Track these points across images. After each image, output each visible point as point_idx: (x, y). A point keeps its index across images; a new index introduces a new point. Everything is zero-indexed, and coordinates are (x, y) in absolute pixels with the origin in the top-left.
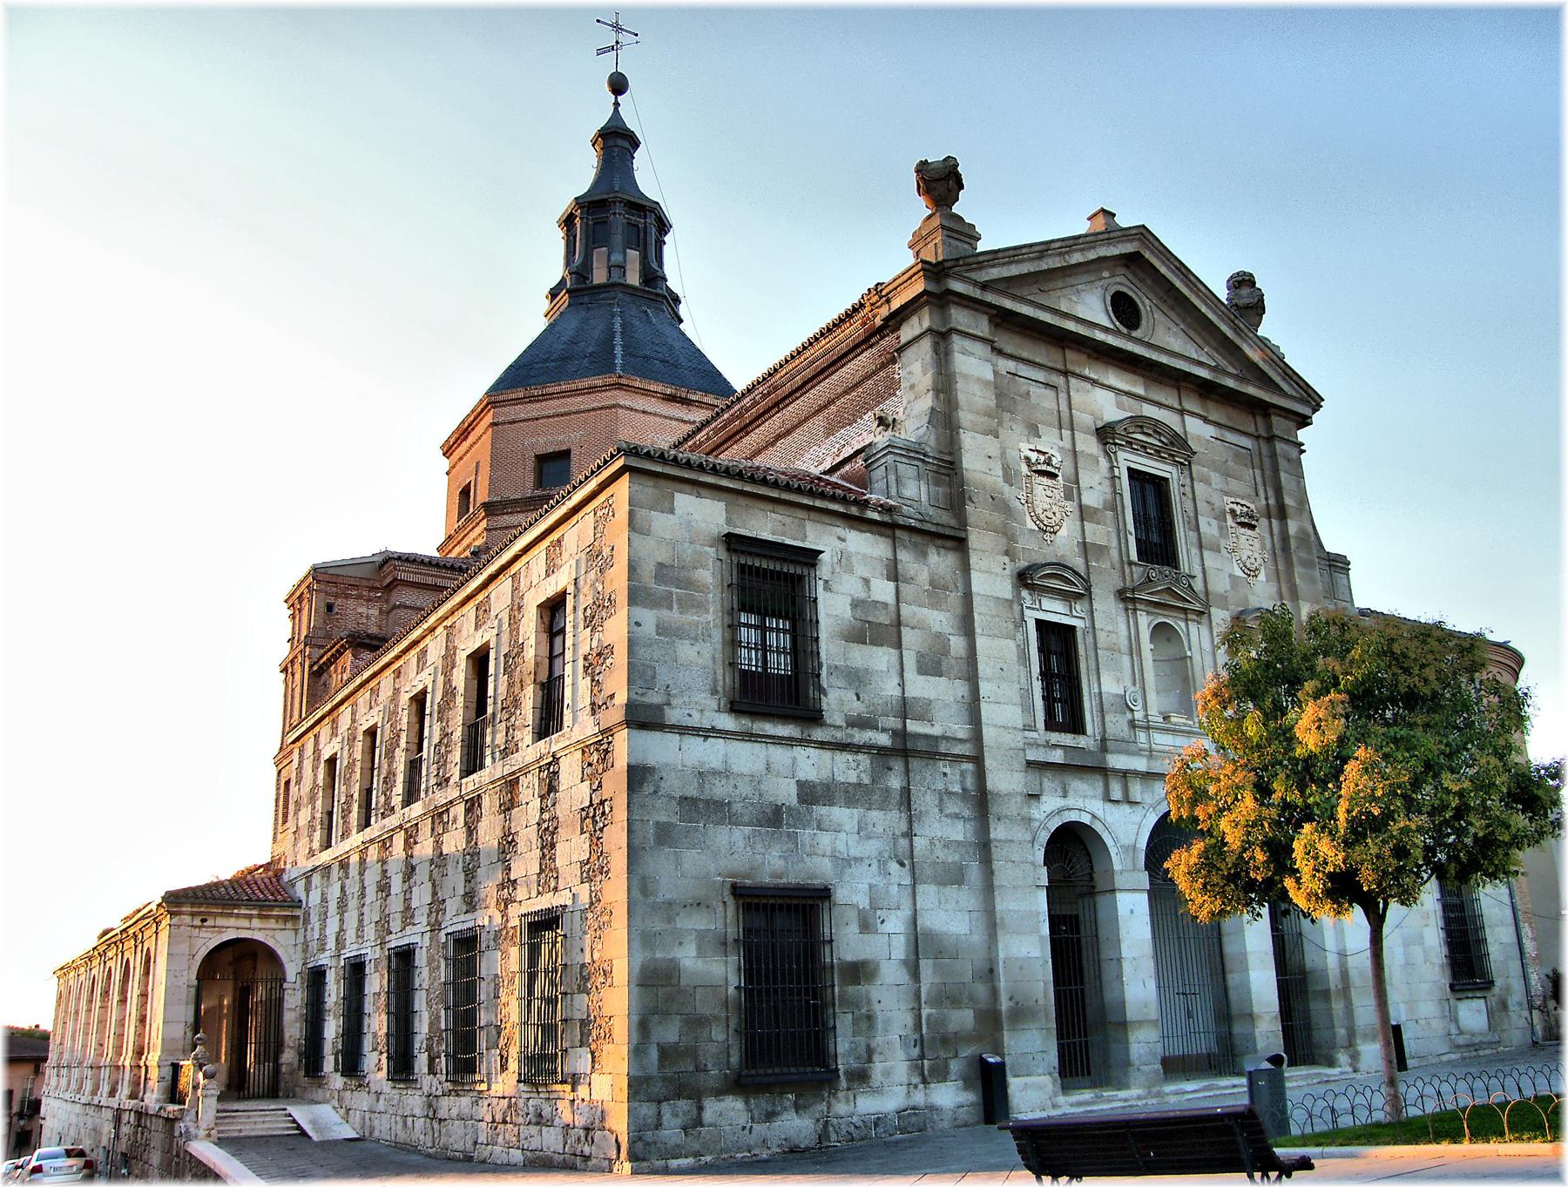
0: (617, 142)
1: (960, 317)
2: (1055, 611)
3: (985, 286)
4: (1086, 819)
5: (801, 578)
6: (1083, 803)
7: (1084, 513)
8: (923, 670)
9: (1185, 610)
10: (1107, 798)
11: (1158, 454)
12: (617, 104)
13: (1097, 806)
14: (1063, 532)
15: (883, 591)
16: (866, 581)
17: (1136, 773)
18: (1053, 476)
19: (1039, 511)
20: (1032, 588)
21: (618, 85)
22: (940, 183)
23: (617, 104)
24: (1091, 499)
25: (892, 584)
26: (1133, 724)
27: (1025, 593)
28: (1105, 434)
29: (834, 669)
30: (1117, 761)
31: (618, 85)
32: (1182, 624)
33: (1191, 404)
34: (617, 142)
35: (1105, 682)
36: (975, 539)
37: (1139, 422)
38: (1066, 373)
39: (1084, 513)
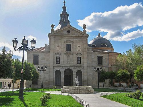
0: (64, 8)
1: (51, 37)
2: (58, 56)
6: (59, 69)
8: (46, 61)
11: (69, 43)
13: (60, 69)
15: (44, 56)
21: (64, 2)
22: (53, 26)
24: (62, 47)
30: (61, 66)
31: (64, 2)
34: (64, 8)
39: (62, 48)
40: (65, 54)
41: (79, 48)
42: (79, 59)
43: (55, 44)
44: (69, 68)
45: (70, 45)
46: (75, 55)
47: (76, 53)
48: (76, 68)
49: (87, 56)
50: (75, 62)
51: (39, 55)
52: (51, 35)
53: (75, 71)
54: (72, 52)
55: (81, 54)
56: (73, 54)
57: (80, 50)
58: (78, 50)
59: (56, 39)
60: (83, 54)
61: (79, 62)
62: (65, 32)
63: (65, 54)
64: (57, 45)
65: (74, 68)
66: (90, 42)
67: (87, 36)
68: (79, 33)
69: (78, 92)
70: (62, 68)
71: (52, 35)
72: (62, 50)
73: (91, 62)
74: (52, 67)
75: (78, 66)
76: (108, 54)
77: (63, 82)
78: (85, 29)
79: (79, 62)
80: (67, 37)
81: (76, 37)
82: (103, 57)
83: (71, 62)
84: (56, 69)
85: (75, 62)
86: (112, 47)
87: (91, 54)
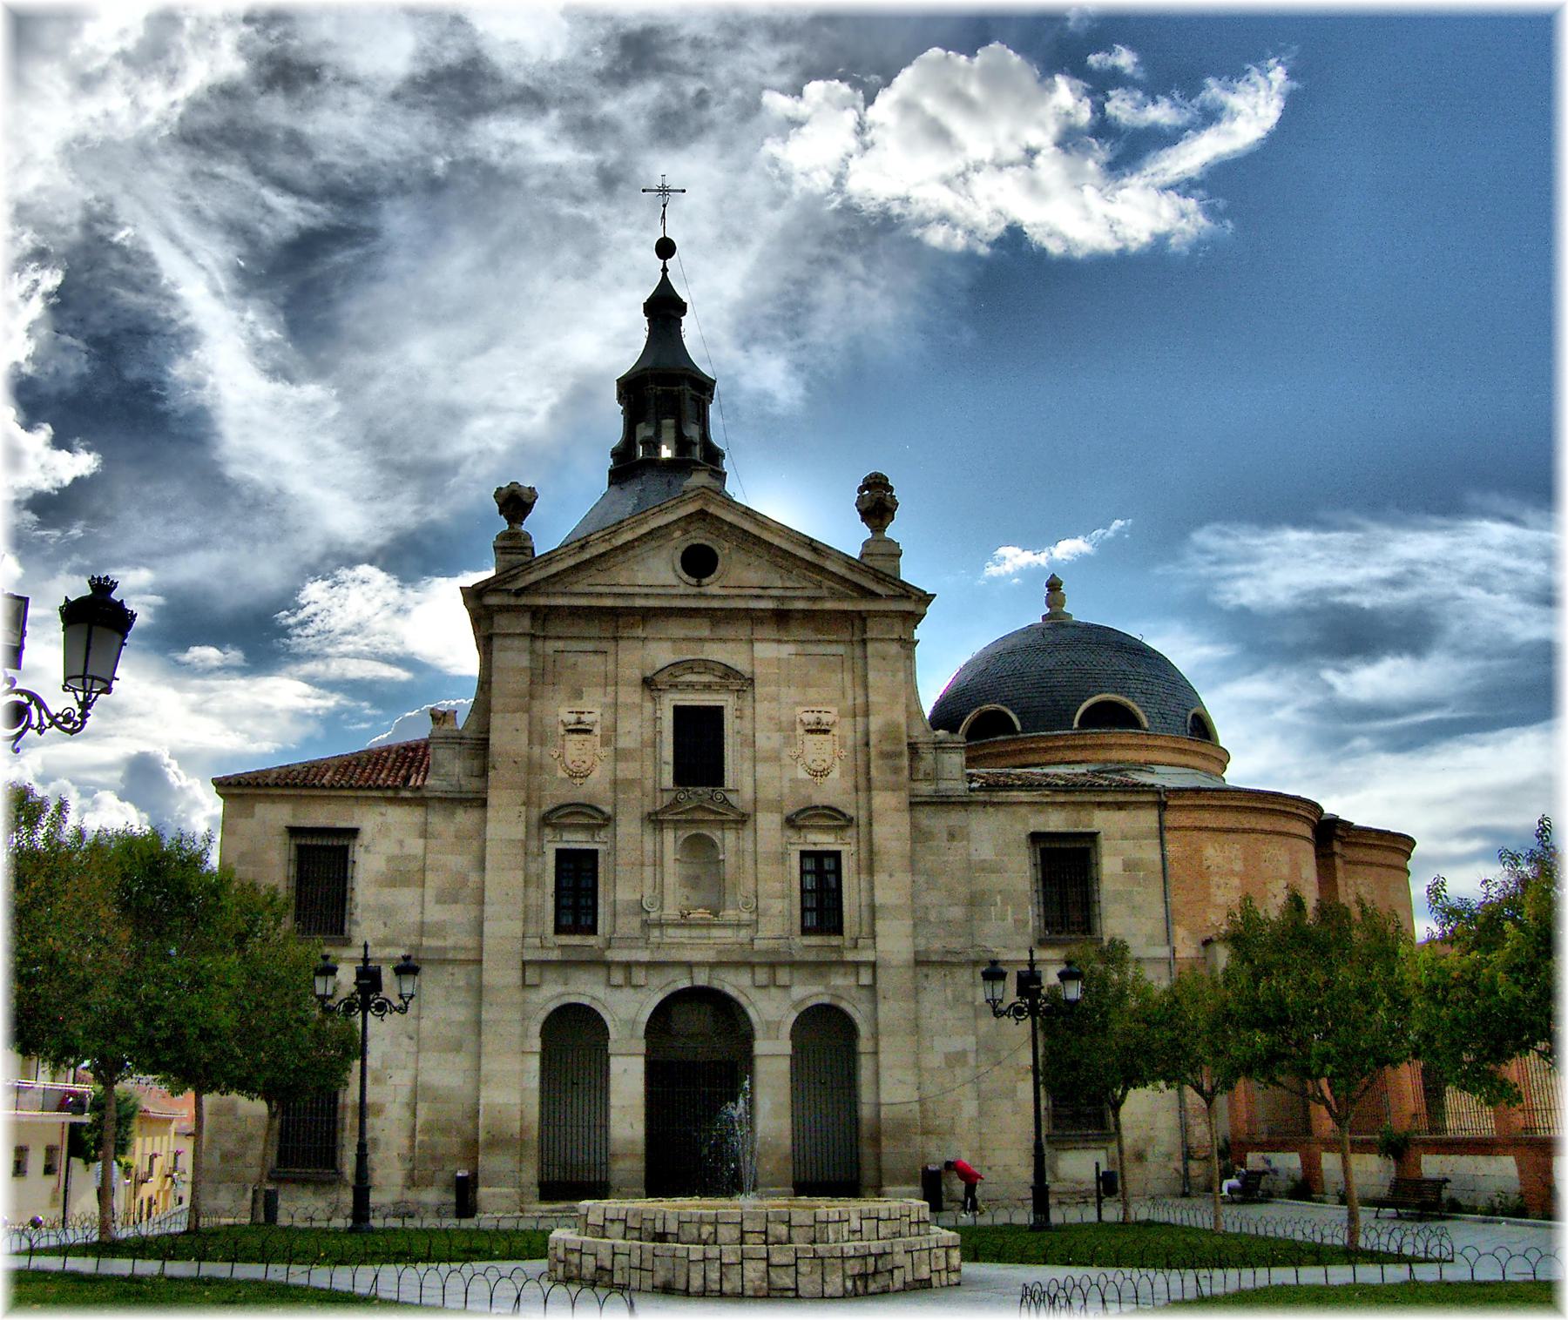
0: (664, 309)
2: (577, 840)
3: (519, 593)
4: (586, 1001)
5: (345, 849)
6: (586, 989)
7: (619, 755)
8: (440, 900)
9: (723, 822)
10: (609, 984)
11: (708, 687)
12: (665, 270)
13: (600, 991)
14: (595, 775)
15: (415, 845)
16: (401, 843)
17: (639, 964)
19: (569, 762)
20: (554, 826)
21: (665, 248)
23: (665, 270)
24: (624, 742)
25: (421, 842)
26: (646, 925)
28: (648, 683)
29: (367, 908)
30: (611, 955)
31: (665, 248)
32: (719, 833)
33: (769, 631)
34: (664, 309)
35: (619, 892)
36: (493, 798)
37: (689, 666)
38: (616, 639)
39: (619, 755)
40: (655, 820)
41: (818, 750)
42: (820, 873)
44: (702, 979)
45: (716, 713)
46: (769, 823)
47: (790, 810)
48: (783, 976)
49: (919, 835)
50: (778, 906)
51: (353, 833)
52: (492, 600)
53: (772, 1013)
54: (732, 798)
55: (833, 817)
56: (743, 820)
57: (824, 773)
58: (802, 774)
59: (551, 646)
60: (863, 821)
61: (822, 902)
62: (659, 573)
63: (655, 820)
65: (762, 976)
66: (940, 661)
67: (908, 606)
68: (821, 570)
69: (754, 1271)
70: (628, 983)
71: (512, 601)
72: (628, 770)
73: (957, 913)
74: (501, 974)
75: (811, 957)
76: (1162, 806)
77: (640, 1148)
78: (891, 532)
79: (822, 902)
80: (676, 629)
81: (781, 618)
82: (1105, 846)
83: (730, 914)
84: (551, 994)
85: (778, 906)
86: (1202, 728)
87: (955, 818)
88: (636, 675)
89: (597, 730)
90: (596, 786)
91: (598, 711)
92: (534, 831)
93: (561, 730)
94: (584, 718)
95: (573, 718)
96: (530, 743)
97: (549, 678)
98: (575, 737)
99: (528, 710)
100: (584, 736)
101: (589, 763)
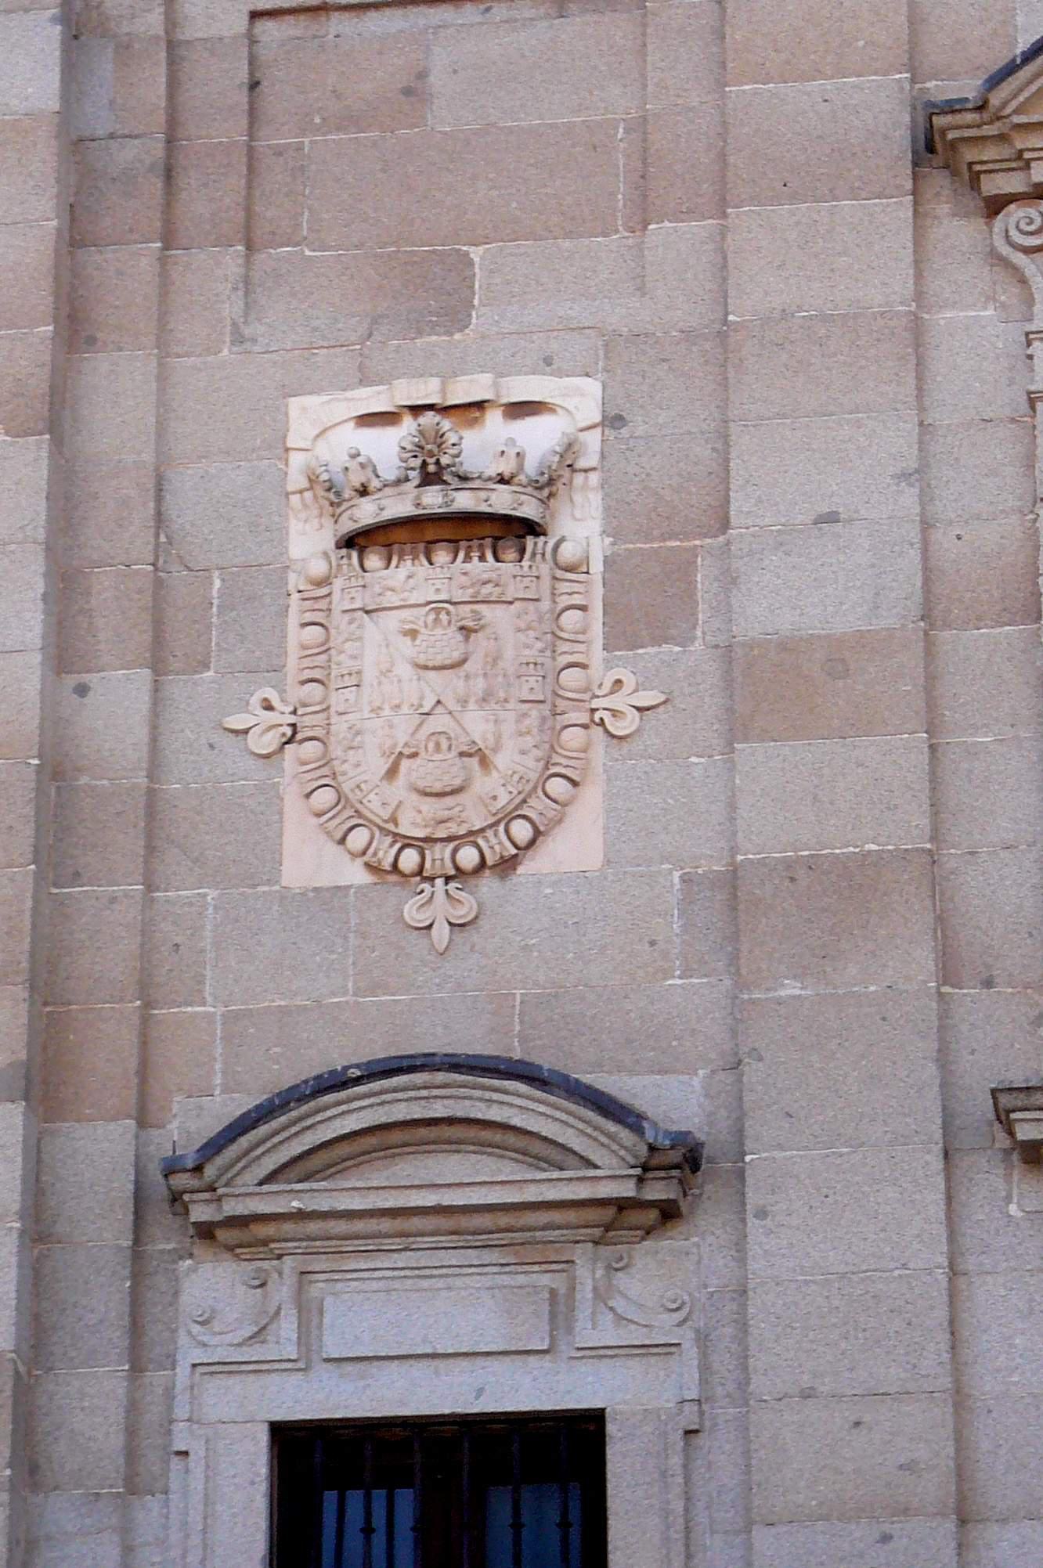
14: (576, 847)
18: (514, 532)
27: (212, 1290)
39: (772, 690)
43: (118, 391)
64: (338, 435)
72: (833, 794)
88: (876, 109)
89: (581, 527)
90: (591, 927)
91: (580, 400)
92: (99, 1299)
93: (309, 542)
94: (481, 446)
95: (386, 448)
96: (66, 654)
97: (208, 197)
98: (415, 579)
99: (57, 416)
100: (480, 568)
101: (514, 759)
